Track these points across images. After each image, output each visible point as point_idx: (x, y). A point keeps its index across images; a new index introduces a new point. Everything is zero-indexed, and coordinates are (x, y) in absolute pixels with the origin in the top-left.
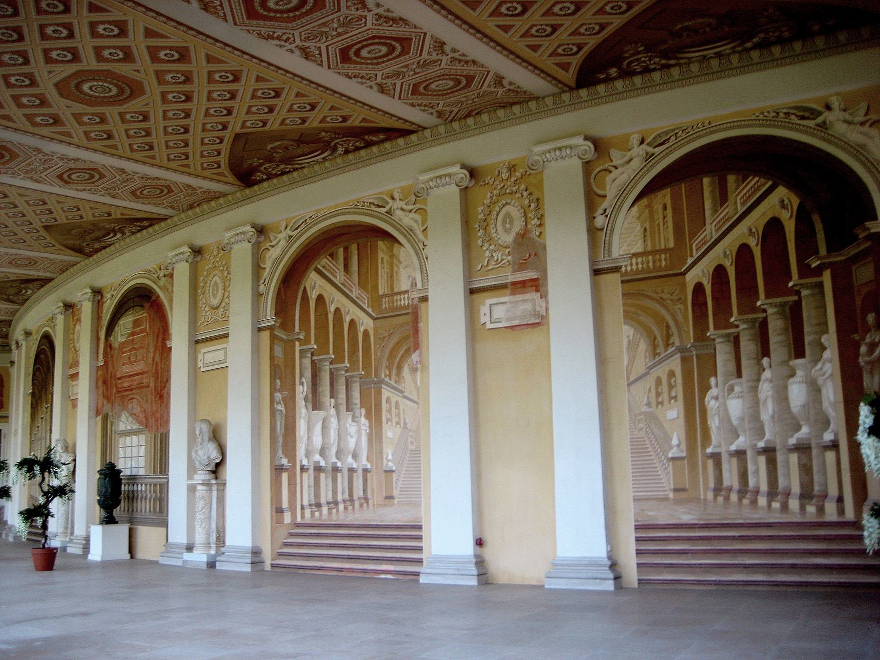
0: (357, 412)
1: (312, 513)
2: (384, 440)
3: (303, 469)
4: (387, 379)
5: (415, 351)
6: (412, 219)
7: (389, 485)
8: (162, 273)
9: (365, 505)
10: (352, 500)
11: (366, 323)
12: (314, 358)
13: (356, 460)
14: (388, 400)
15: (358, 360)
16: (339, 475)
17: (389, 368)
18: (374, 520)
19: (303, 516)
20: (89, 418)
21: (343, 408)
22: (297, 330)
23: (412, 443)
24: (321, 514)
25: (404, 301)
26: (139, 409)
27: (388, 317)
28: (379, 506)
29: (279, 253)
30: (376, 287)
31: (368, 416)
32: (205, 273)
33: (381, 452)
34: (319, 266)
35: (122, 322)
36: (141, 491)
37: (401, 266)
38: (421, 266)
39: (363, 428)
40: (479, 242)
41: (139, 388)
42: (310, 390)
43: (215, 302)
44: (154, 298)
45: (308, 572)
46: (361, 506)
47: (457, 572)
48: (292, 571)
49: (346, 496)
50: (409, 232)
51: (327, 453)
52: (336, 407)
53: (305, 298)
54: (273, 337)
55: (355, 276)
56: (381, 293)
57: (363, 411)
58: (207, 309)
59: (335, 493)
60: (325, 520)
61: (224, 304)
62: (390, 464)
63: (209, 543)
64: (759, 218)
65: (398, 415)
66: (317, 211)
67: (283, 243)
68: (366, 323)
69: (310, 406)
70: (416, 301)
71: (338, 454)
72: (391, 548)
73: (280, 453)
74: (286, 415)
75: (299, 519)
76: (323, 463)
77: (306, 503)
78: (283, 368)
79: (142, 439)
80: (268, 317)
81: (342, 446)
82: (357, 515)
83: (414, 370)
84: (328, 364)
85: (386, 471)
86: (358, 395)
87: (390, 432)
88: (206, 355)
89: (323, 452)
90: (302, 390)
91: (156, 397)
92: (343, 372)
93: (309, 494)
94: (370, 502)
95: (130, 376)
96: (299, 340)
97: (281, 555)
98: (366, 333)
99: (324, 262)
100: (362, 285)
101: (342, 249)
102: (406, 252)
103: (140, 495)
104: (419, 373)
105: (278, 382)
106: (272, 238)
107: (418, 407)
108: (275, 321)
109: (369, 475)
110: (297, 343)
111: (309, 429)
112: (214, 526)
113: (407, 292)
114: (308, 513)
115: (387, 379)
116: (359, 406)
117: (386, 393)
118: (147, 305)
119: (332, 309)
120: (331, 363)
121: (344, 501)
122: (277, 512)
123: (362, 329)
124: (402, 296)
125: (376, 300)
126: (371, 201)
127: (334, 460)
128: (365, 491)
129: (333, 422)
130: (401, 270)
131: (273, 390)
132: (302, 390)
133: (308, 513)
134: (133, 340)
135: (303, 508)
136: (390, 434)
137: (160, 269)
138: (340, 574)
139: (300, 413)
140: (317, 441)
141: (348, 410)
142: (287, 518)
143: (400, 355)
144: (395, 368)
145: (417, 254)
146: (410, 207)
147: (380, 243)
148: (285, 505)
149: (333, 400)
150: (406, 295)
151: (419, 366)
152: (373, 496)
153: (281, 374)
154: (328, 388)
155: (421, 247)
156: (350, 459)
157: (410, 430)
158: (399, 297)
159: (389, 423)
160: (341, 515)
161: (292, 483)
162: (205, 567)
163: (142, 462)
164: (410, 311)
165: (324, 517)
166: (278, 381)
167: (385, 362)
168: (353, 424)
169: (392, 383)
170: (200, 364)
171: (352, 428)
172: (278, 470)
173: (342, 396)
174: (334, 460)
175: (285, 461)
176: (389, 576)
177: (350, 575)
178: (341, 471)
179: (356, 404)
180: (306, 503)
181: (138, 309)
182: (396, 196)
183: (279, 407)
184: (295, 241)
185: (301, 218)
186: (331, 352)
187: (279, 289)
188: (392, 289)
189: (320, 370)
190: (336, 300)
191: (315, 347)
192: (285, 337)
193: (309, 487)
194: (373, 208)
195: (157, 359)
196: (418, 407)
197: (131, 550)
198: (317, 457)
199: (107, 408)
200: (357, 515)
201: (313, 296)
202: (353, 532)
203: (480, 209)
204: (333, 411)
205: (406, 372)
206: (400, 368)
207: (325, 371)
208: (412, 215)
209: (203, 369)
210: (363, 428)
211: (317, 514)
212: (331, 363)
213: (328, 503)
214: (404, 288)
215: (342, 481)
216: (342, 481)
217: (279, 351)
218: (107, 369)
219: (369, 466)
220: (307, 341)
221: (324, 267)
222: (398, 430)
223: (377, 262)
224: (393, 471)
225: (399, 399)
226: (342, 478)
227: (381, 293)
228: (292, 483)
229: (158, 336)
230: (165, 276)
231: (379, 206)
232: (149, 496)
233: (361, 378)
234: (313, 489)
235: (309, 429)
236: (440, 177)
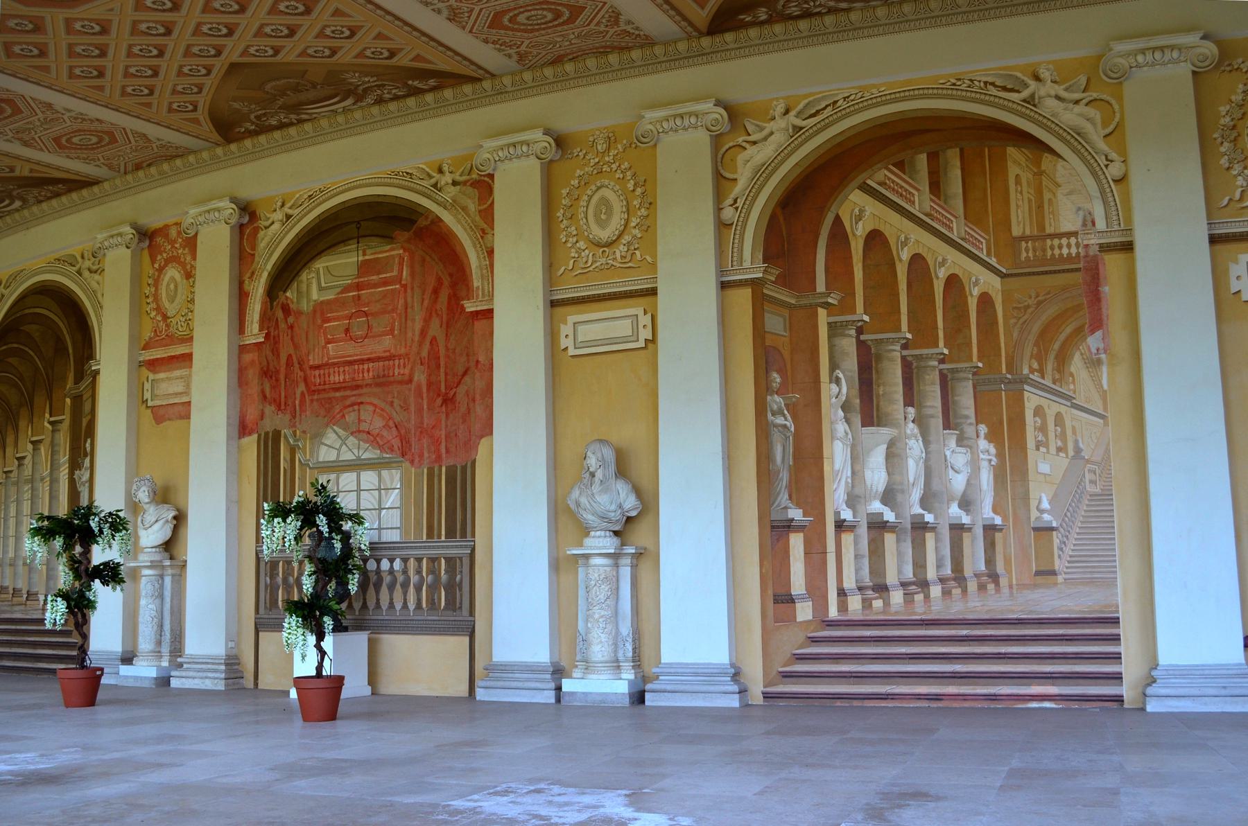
0: (970, 431)
1: (867, 604)
2: (1031, 475)
3: (840, 526)
4: (1035, 377)
5: (1092, 332)
6: (1080, 115)
7: (1045, 552)
8: (448, 178)
9: (991, 587)
10: (959, 576)
11: (982, 281)
12: (863, 337)
13: (967, 511)
14: (1039, 412)
15: (969, 345)
16: (930, 537)
17: (1040, 358)
18: (1013, 612)
19: (843, 607)
20: (229, 438)
21: (939, 421)
22: (821, 287)
23: (1091, 482)
24: (887, 604)
25: (1068, 249)
26: (378, 423)
27: (1034, 274)
28: (1022, 586)
29: (769, 157)
30: (1005, 223)
31: (993, 437)
32: (575, 182)
33: (1026, 498)
34: (869, 182)
35: (320, 264)
36: (391, 571)
37: (1060, 193)
38: (1103, 193)
39: (982, 456)
40: (1224, 161)
41: (378, 385)
42: (855, 391)
43: (604, 234)
44: (422, 222)
45: (856, 703)
46: (982, 587)
47: (1223, 692)
48: (817, 703)
49: (948, 571)
50: (1075, 138)
51: (899, 498)
52: (920, 421)
53: (839, 235)
54: (760, 302)
55: (958, 204)
56: (1016, 231)
57: (983, 429)
58: (582, 245)
59: (919, 565)
60: (896, 613)
61: (626, 238)
62: (1046, 517)
63: (617, 661)
65: (1063, 436)
66: (862, 89)
67: (779, 139)
68: (982, 281)
69: (857, 420)
70: (1094, 251)
71: (925, 502)
72: (1052, 657)
73: (784, 498)
74: (796, 435)
75: (833, 613)
76: (889, 516)
77: (849, 583)
78: (786, 354)
79: (393, 477)
80: (747, 264)
81: (936, 485)
82: (971, 604)
83: (1093, 363)
84: (898, 348)
85: (1035, 529)
86: (972, 402)
87: (1044, 466)
88: (580, 328)
89: (888, 497)
90: (836, 393)
91: (431, 401)
92: (936, 363)
93: (857, 571)
94: (1003, 581)
95: (351, 363)
96: (827, 305)
97: (787, 676)
98: (985, 300)
99: (880, 175)
100: (973, 216)
101: (922, 159)
102: (1069, 169)
103: (387, 579)
104: (1104, 369)
105: (776, 378)
106: (750, 128)
107: (1106, 424)
108: (765, 271)
109: (998, 535)
110: (822, 313)
111: (857, 458)
112: (626, 628)
113: (1075, 234)
114: (855, 603)
115: (1035, 377)
116: (973, 420)
117: (1032, 399)
118: (403, 236)
119: (905, 255)
120: (905, 347)
121: (942, 580)
122: (776, 601)
123: (976, 292)
124: (1064, 241)
125: (1008, 244)
126: (990, 79)
127: (918, 510)
128: (990, 561)
129: (915, 447)
130: (1060, 196)
131: (762, 390)
132: (836, 393)
133: (855, 603)
134: (359, 297)
135: (842, 593)
136: (1044, 468)
137: (440, 171)
138: (934, 705)
139: (833, 431)
140: (876, 476)
141: (947, 425)
142: (804, 611)
143: (1062, 337)
144: (1052, 356)
145: (1094, 174)
146: (1076, 96)
147: (1012, 151)
148: (798, 584)
149: (911, 410)
150: (1073, 240)
151: (1103, 356)
152: (1009, 571)
153: (778, 368)
154: (900, 389)
155: (1102, 161)
156: (954, 510)
157: (1088, 461)
158: (1056, 242)
159: (1043, 449)
160: (936, 603)
161: (815, 554)
162: (626, 702)
163: (392, 518)
164: (1081, 265)
165: (893, 609)
166: (775, 375)
167: (1029, 349)
168: (963, 450)
169: (1048, 382)
170: (564, 343)
172: (776, 531)
173: (934, 402)
174: (918, 510)
175: (796, 514)
176: (1047, 705)
177: (956, 705)
178: (933, 529)
179: (967, 417)
180: (849, 583)
181: (374, 241)
182: (1045, 74)
183: (780, 420)
184: (806, 141)
185: (823, 98)
186: (904, 327)
187: (773, 217)
188: (1042, 227)
189: (879, 358)
190: (908, 240)
191: (866, 318)
192: (793, 302)
193: (857, 557)
194: (993, 91)
195: (435, 329)
196: (1106, 424)
197: (373, 679)
198: (876, 506)
199: (274, 420)
200: (971, 604)
201: (858, 233)
202: (964, 632)
203: (1223, 109)
204: (911, 428)
205: (1076, 365)
206: (1062, 360)
207: (892, 360)
208: (1077, 109)
209: (571, 352)
210: (982, 456)
211: (877, 604)
212: (905, 347)
213: (904, 585)
214: (1067, 227)
215: (936, 550)
216: (936, 550)
217: (775, 323)
218: (275, 352)
219: (998, 521)
220: (847, 305)
221: (880, 184)
222: (1063, 462)
223: (1006, 181)
224: (1052, 529)
225: (1063, 409)
226: (938, 540)
227: (1016, 231)
228: (815, 554)
229: (436, 292)
230: (455, 183)
231: (1005, 89)
232: (414, 579)
233: (974, 374)
234: (866, 561)
235: (857, 458)
236: (1161, 49)
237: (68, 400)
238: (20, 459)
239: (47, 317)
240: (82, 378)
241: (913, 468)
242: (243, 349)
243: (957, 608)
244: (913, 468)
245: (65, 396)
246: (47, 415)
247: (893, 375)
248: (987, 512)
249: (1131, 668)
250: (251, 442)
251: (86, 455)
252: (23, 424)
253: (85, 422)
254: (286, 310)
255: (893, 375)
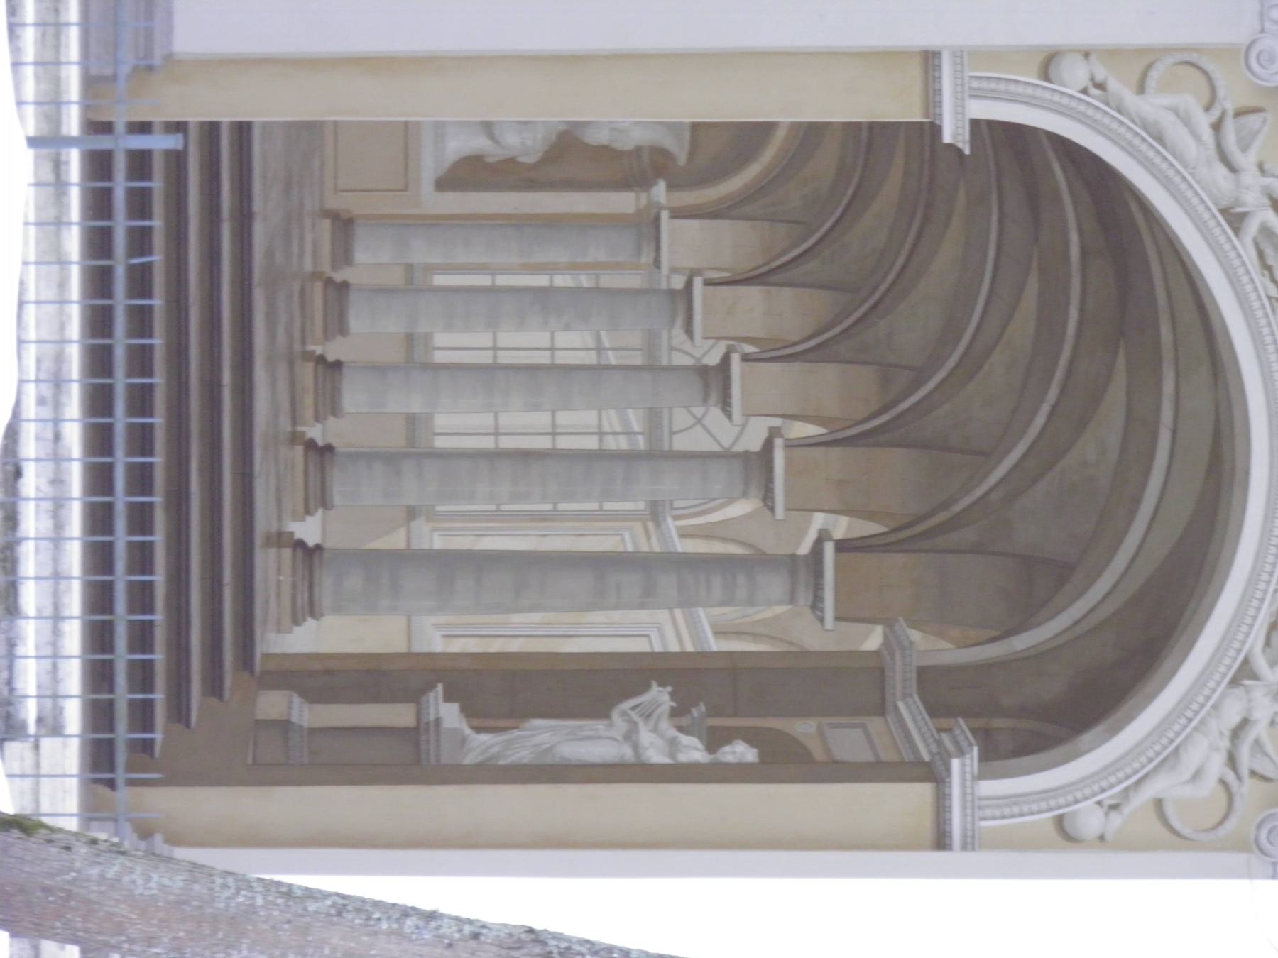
237: (873, 640)
238: (714, 381)
239: (1137, 501)
240: (938, 708)
245: (889, 624)
246: (842, 527)
251: (714, 740)
252: (830, 385)
253: (803, 728)
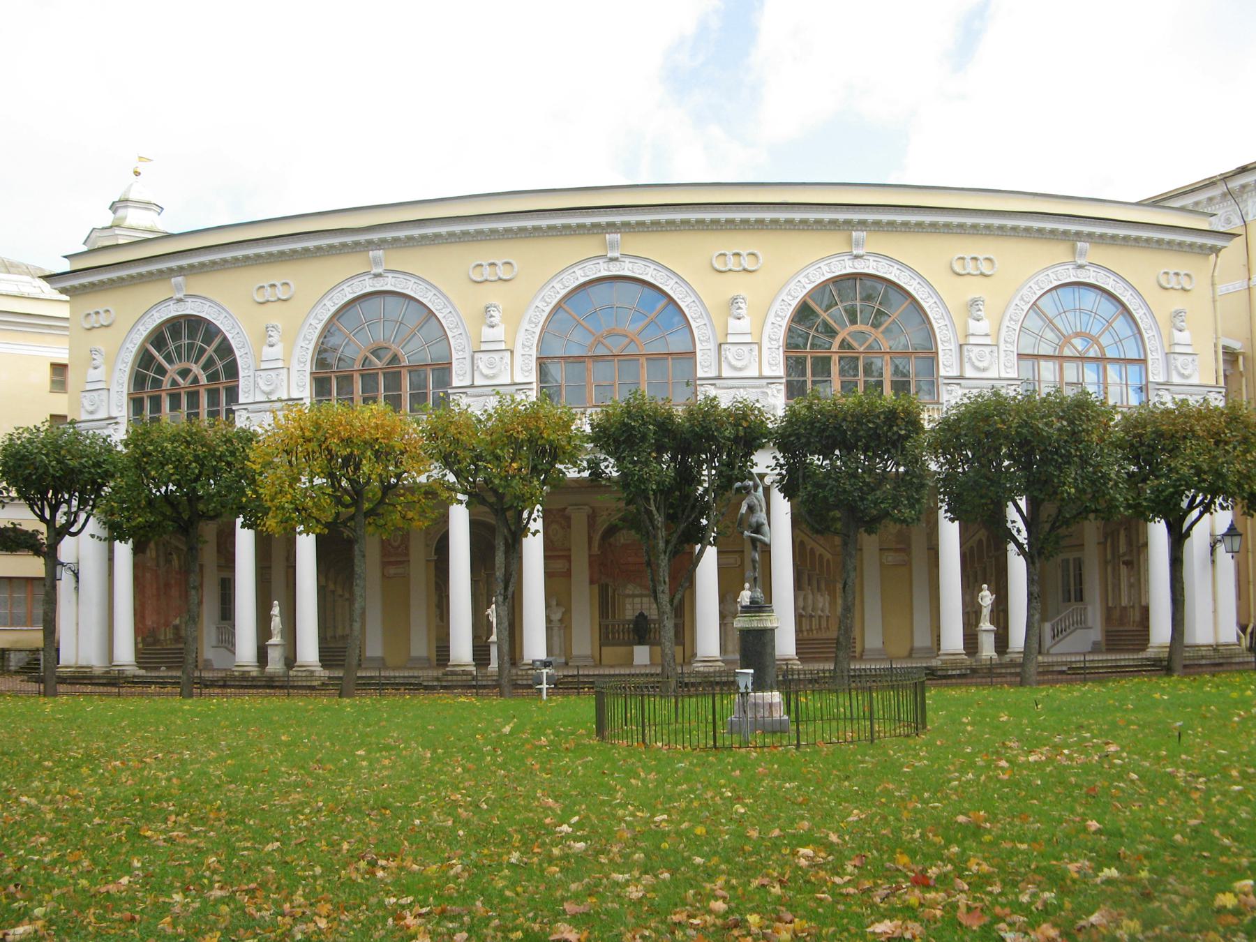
11: (827, 556)
64: (977, 538)
68: (827, 556)
89: (804, 609)
129: (810, 597)
160: (815, 635)
171: (820, 599)
173: (815, 585)
215: (815, 622)
241: (810, 602)
242: (590, 556)
243: (820, 636)
244: (810, 602)
247: (806, 578)
248: (827, 612)
249: (858, 649)
250: (596, 587)
254: (610, 545)
255: (806, 578)
